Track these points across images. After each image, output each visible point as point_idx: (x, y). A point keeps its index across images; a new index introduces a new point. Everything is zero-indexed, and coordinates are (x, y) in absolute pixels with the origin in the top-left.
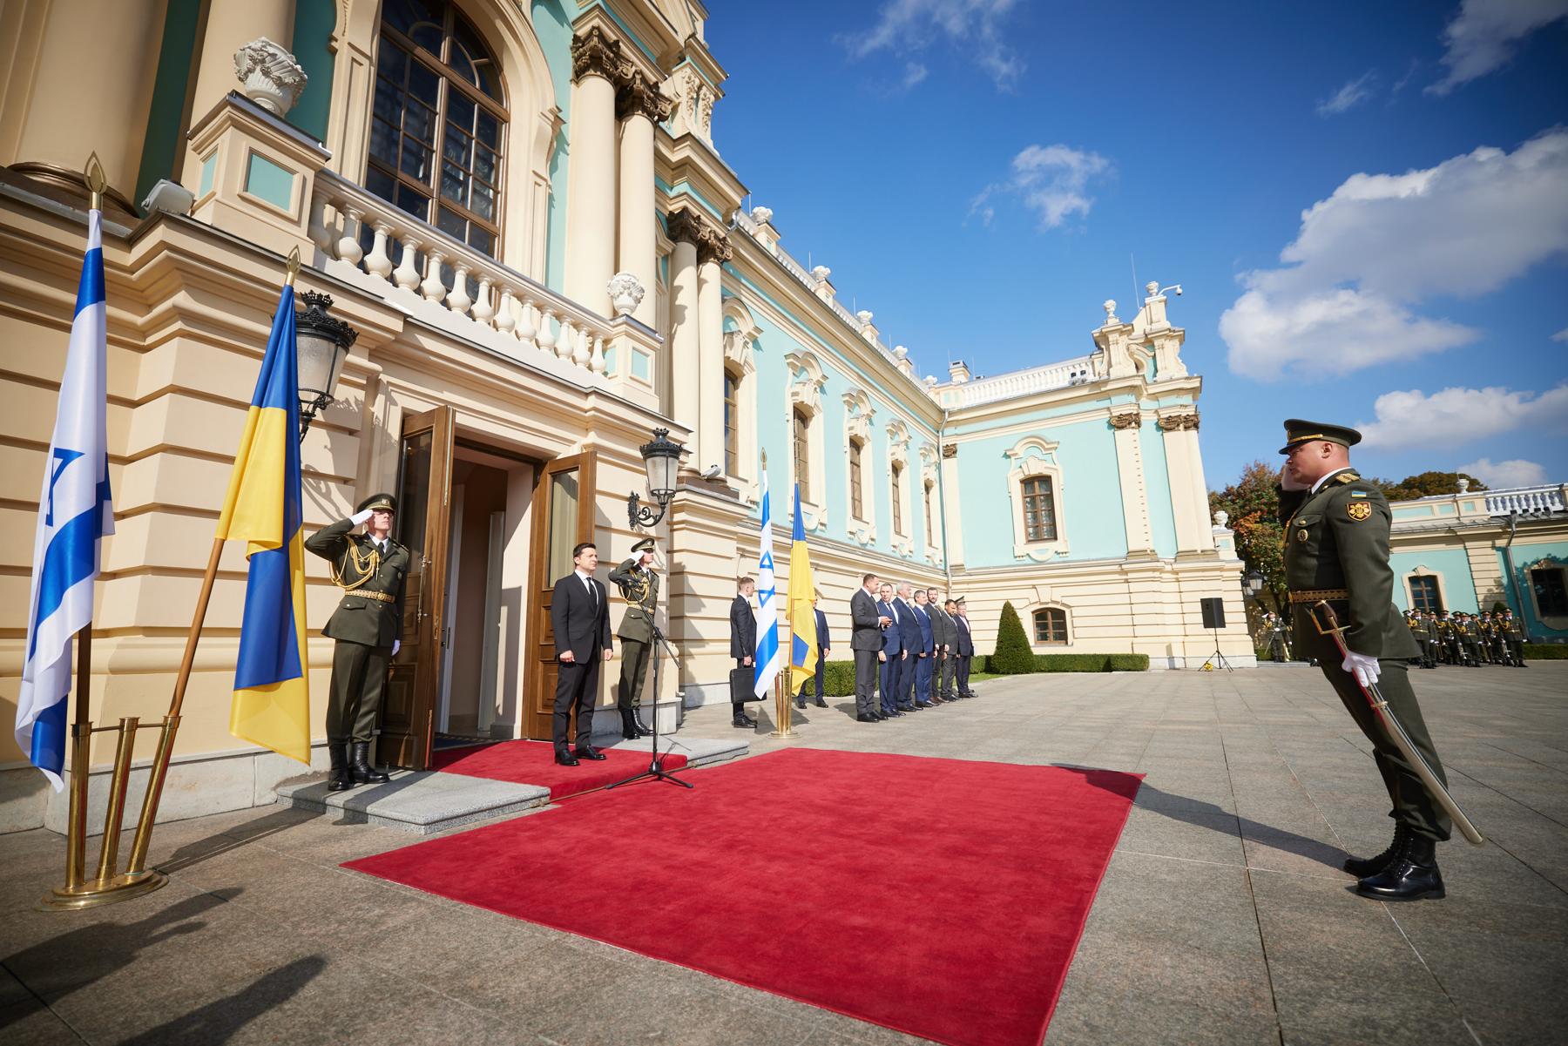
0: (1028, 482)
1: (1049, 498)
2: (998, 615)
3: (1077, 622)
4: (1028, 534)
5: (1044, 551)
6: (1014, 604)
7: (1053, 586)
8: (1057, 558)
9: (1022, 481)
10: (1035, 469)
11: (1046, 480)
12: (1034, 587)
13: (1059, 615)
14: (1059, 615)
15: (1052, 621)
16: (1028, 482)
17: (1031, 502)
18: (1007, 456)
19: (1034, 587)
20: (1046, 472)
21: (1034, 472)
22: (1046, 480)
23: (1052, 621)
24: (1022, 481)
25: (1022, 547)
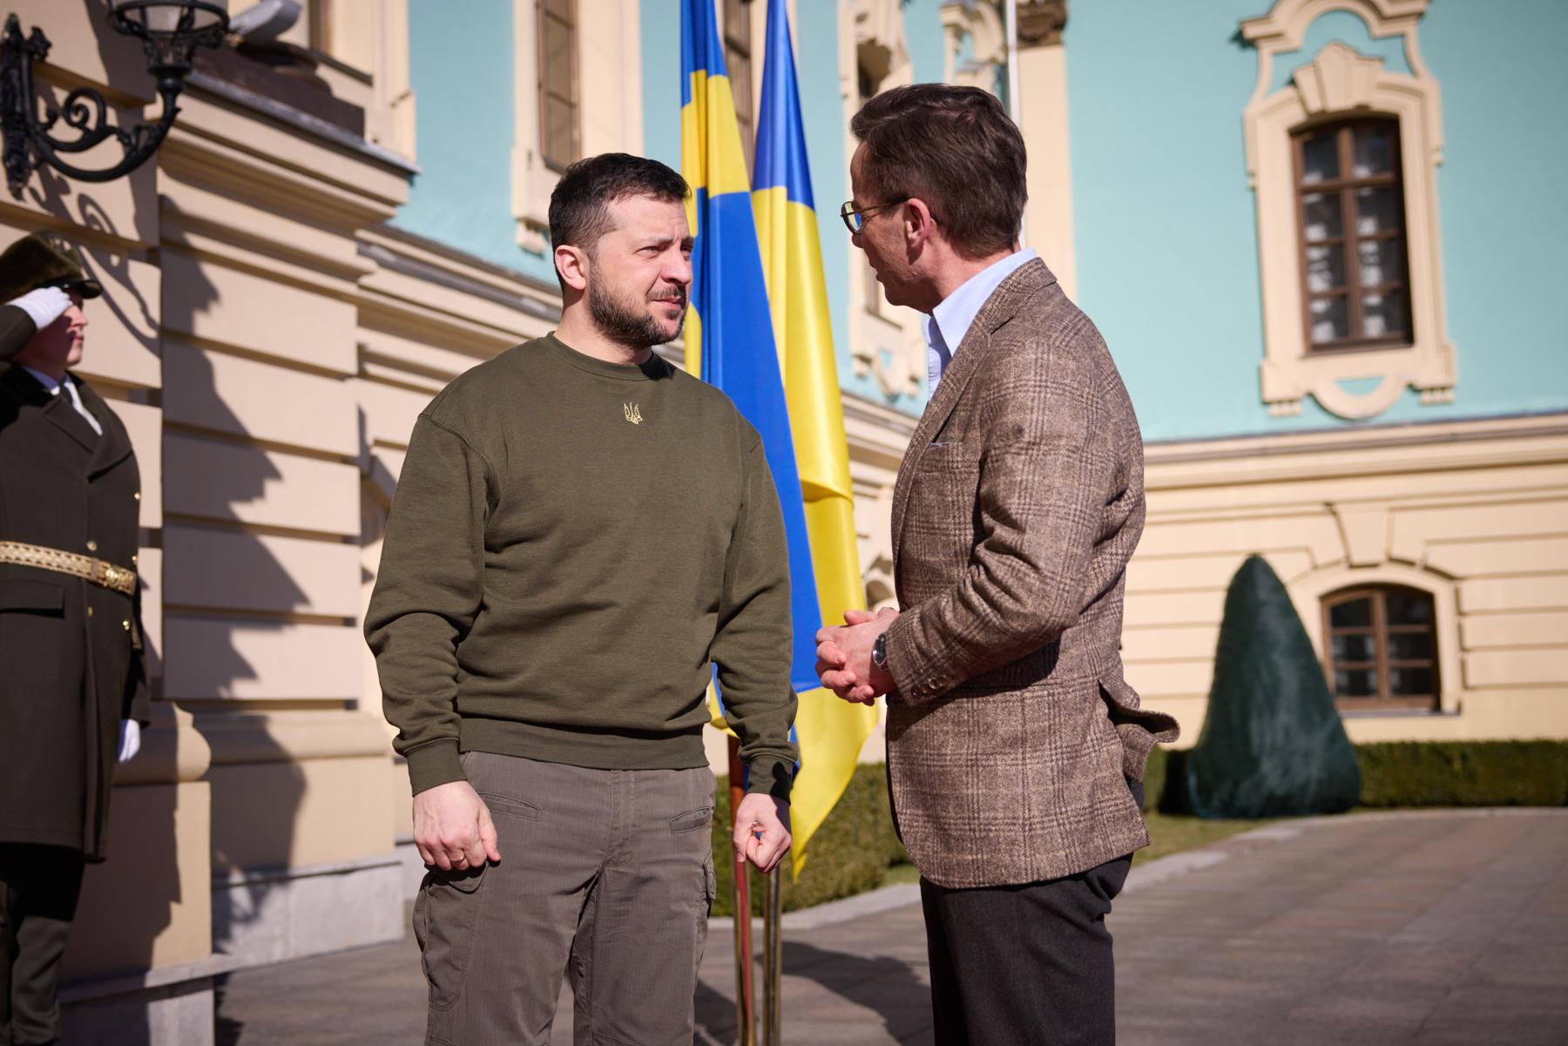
0: (1317, 138)
1: (1389, 200)
2: (1213, 609)
3: (1475, 631)
4: (1311, 320)
5: (1370, 380)
6: (1285, 568)
7: (1397, 506)
8: (1412, 408)
9: (1295, 133)
10: (1345, 87)
11: (1379, 131)
12: (1330, 507)
13: (1411, 608)
14: (1411, 608)
15: (1395, 629)
16: (1317, 138)
17: (1322, 207)
18: (1243, 41)
19: (1330, 507)
20: (1381, 102)
21: (1339, 100)
22: (1379, 131)
23: (1395, 629)
24: (1295, 133)
25: (1289, 368)
